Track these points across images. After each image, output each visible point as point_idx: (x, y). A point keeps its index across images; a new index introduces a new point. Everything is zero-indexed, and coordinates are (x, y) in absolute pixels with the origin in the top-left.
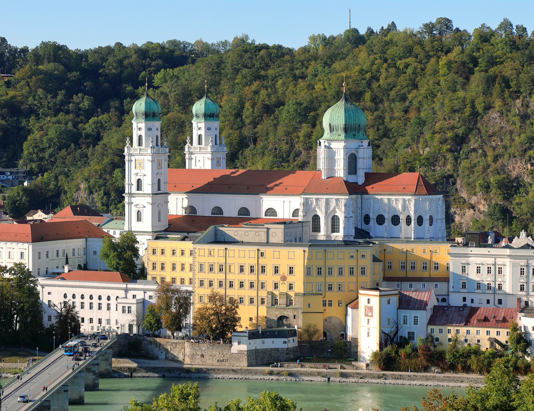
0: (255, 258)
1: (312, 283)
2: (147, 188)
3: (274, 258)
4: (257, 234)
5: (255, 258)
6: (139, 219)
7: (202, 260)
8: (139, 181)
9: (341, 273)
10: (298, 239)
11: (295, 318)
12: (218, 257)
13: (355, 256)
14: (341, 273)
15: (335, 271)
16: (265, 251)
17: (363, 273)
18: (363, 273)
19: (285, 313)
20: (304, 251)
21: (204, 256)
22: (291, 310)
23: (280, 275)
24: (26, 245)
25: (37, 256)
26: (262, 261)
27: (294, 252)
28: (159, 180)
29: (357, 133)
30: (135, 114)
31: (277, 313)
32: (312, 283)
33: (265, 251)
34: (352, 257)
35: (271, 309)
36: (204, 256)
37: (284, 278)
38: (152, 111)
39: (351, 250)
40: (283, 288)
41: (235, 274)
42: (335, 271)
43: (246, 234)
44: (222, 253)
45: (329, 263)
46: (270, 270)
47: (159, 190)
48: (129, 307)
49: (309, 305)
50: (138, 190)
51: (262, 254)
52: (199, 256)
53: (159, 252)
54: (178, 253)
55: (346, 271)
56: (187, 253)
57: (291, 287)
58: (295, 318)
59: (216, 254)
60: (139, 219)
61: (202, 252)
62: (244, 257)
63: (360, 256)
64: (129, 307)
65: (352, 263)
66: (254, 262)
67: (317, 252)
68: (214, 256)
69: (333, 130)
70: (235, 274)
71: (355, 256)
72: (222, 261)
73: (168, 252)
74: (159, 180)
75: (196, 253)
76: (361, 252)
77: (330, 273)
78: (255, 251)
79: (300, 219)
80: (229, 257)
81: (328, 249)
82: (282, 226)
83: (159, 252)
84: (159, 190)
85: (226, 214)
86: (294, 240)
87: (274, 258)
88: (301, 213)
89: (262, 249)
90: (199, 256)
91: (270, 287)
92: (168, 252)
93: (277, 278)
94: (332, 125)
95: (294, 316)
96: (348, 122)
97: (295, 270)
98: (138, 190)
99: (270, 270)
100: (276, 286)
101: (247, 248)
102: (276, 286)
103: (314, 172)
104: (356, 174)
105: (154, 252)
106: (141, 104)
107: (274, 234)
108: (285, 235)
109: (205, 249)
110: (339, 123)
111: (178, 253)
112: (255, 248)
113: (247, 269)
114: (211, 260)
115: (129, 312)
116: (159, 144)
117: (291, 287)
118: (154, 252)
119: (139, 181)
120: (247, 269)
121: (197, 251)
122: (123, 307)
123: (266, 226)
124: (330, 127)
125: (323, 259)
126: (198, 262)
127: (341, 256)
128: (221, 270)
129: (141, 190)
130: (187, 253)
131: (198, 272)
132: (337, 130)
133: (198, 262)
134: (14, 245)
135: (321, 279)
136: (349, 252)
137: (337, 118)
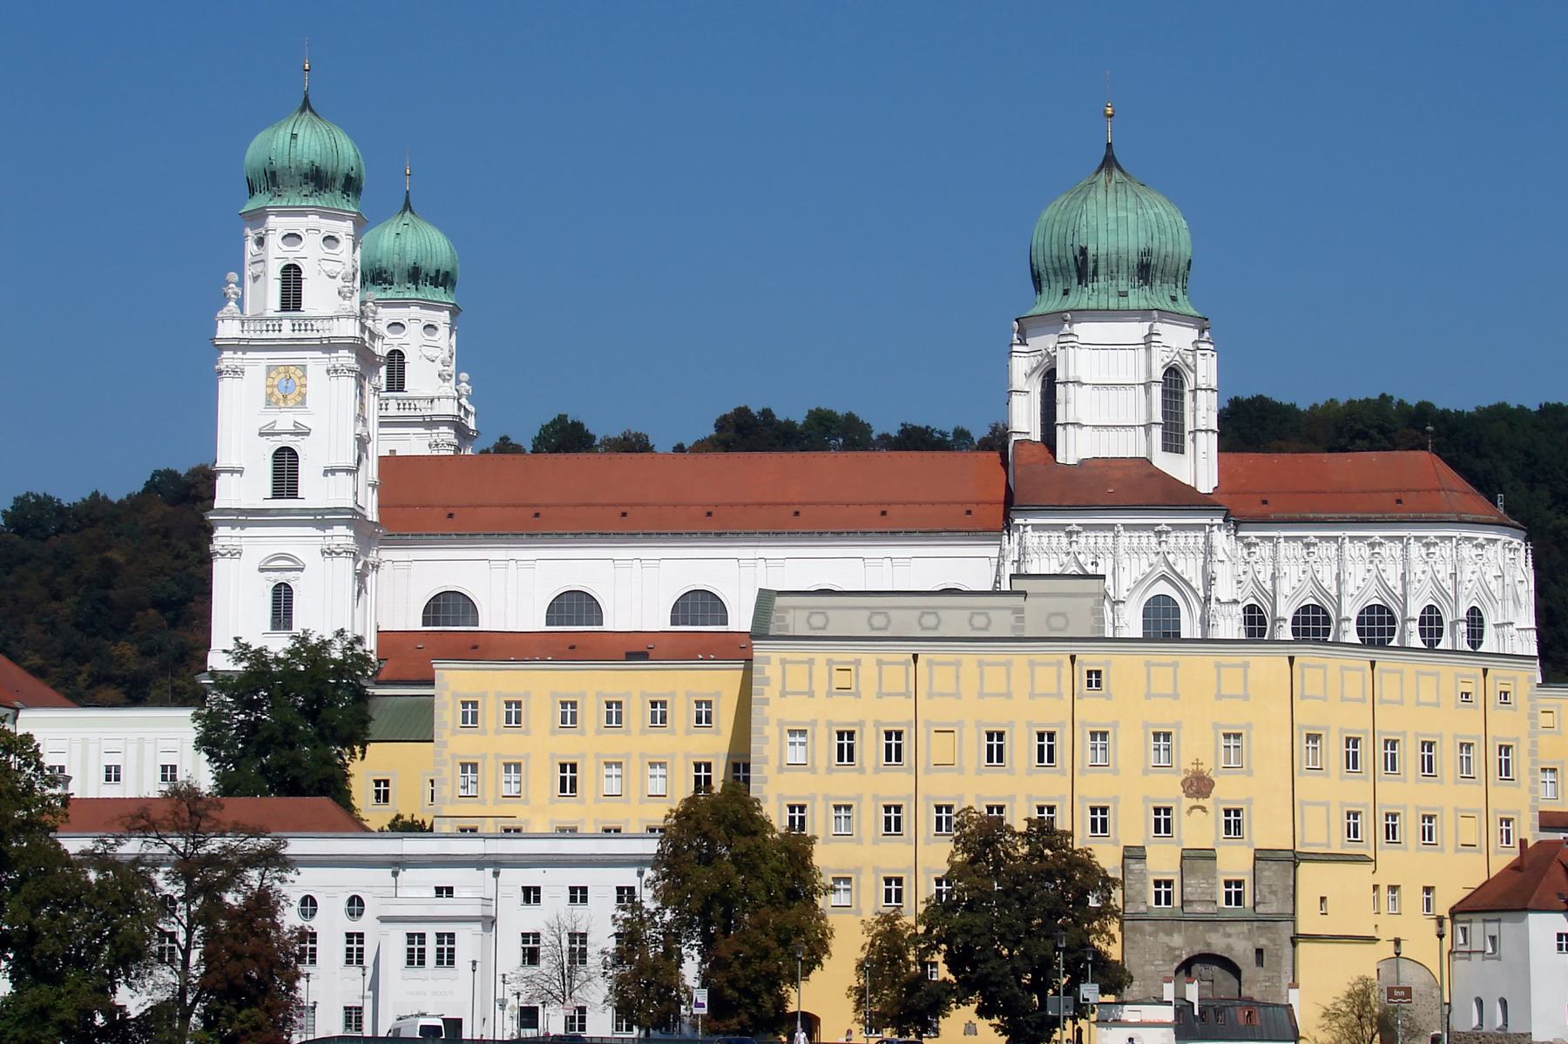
0: (1059, 695)
1: (1327, 804)
3: (1148, 696)
5: (1059, 695)
7: (798, 711)
11: (1260, 962)
12: (880, 695)
13: (1477, 697)
15: (1410, 756)
16: (1107, 664)
19: (1217, 942)
20: (1291, 659)
21: (811, 694)
22: (1245, 927)
23: (1177, 772)
26: (1093, 710)
27: (1246, 666)
29: (1179, 291)
31: (1177, 940)
32: (1327, 804)
33: (1107, 664)
35: (1147, 926)
36: (811, 694)
37: (1199, 785)
38: (344, 168)
40: (1199, 828)
41: (961, 770)
42: (1410, 756)
44: (896, 677)
45: (1389, 724)
46: (1130, 745)
48: (440, 936)
49: (1323, 899)
50: (277, 494)
52: (784, 693)
53: (492, 713)
54: (591, 714)
55: (1446, 758)
57: (1233, 823)
58: (1260, 962)
61: (797, 678)
62: (1008, 695)
63: (1493, 697)
64: (440, 936)
65: (1467, 723)
66: (1053, 716)
67: (1343, 668)
68: (858, 695)
69: (1095, 273)
70: (961, 770)
72: (897, 714)
76: (1496, 678)
78: (1060, 664)
80: (930, 695)
83: (492, 713)
85: (615, 619)
87: (1148, 696)
89: (1091, 658)
90: (784, 693)
91: (1131, 826)
92: (542, 714)
93: (1168, 788)
94: (1091, 251)
95: (1259, 952)
96: (1156, 241)
97: (1255, 743)
98: (277, 494)
99: (1130, 745)
100: (1163, 822)
101: (1019, 657)
102: (1163, 822)
104: (1180, 450)
106: (294, 136)
109: (811, 662)
110: (1122, 244)
112: (1061, 653)
113: (1021, 748)
114: (845, 713)
115: (446, 958)
117: (1233, 823)
120: (1021, 748)
122: (410, 936)
125: (1363, 700)
126: (781, 723)
128: (894, 753)
129: (293, 494)
131: (780, 770)
132: (1111, 275)
133: (781, 723)
135: (1356, 792)
136: (1457, 676)
137: (1112, 226)
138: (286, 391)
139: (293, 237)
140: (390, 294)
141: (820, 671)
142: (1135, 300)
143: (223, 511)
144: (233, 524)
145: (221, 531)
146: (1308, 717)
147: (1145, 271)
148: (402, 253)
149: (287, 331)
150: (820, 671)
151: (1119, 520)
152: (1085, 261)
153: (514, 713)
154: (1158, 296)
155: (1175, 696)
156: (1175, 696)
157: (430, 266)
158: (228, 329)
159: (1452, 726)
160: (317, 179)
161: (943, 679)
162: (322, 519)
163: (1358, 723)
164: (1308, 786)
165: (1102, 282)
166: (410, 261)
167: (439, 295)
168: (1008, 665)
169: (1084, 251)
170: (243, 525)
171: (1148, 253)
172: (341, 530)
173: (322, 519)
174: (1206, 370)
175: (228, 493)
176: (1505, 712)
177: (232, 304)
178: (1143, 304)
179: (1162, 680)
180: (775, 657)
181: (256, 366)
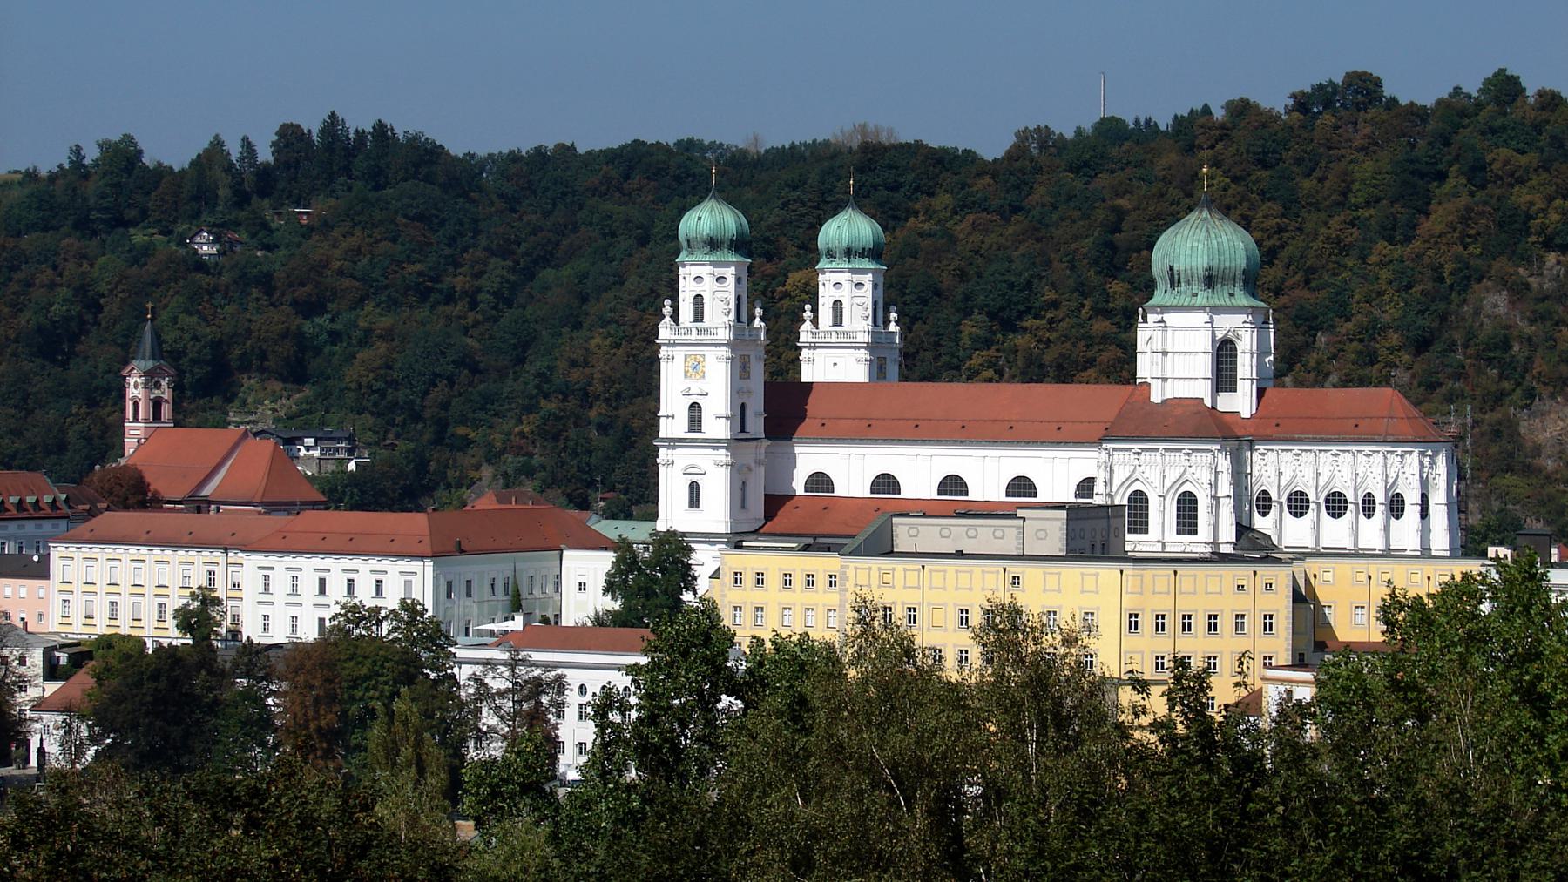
2: (717, 426)
4: (999, 534)
6: (694, 501)
8: (695, 411)
9: (1212, 627)
10: (1098, 546)
13: (1249, 587)
14: (1212, 627)
15: (1200, 623)
17: (1268, 627)
18: (1268, 627)
24: (416, 565)
25: (446, 589)
27: (1097, 575)
28: (743, 406)
30: (685, 244)
34: (1240, 587)
39: (1242, 573)
42: (1200, 623)
43: (972, 533)
44: (913, 578)
45: (1185, 606)
47: (743, 430)
50: (691, 430)
51: (1016, 580)
53: (749, 579)
54: (799, 581)
55: (1226, 623)
56: (821, 581)
59: (899, 582)
60: (694, 501)
62: (970, 589)
63: (1260, 586)
65: (1243, 603)
71: (1249, 587)
72: (913, 598)
73: (774, 580)
74: (743, 406)
75: (847, 579)
77: (1186, 627)
79: (1098, 500)
81: (1183, 570)
82: (1063, 514)
83: (749, 579)
84: (743, 430)
86: (1088, 546)
88: (1099, 487)
89: (1015, 568)
92: (774, 580)
98: (691, 430)
103: (1130, 388)
105: (738, 579)
107: (1041, 534)
108: (1071, 535)
111: (799, 581)
112: (998, 565)
116: (744, 317)
118: (738, 579)
119: (695, 411)
121: (850, 573)
123: (1020, 513)
124: (1172, 275)
127: (1213, 585)
130: (821, 581)
132: (1188, 283)
134: (385, 564)
138: (695, 369)
139: (698, 278)
140: (834, 265)
141: (874, 573)
142: (1201, 300)
143: (663, 440)
144: (668, 447)
145: (662, 451)
146: (1130, 604)
147: (1210, 280)
148: (840, 239)
149: (694, 335)
150: (874, 573)
151: (1161, 446)
152: (1172, 275)
153: (760, 580)
154: (1221, 298)
155: (1059, 591)
156: (1059, 591)
157: (859, 246)
158: (664, 332)
159: (1227, 606)
160: (713, 244)
161: (937, 579)
162: (714, 444)
163: (1164, 605)
164: (1131, 641)
165: (1183, 287)
166: (845, 244)
167: (867, 264)
168: (971, 572)
169: (1171, 268)
170: (674, 448)
171: (1210, 269)
172: (723, 452)
173: (714, 444)
174: (1246, 342)
175: (666, 429)
176: (1269, 595)
177: (667, 319)
178: (1205, 302)
179: (1052, 582)
180: (852, 566)
181: (680, 352)
